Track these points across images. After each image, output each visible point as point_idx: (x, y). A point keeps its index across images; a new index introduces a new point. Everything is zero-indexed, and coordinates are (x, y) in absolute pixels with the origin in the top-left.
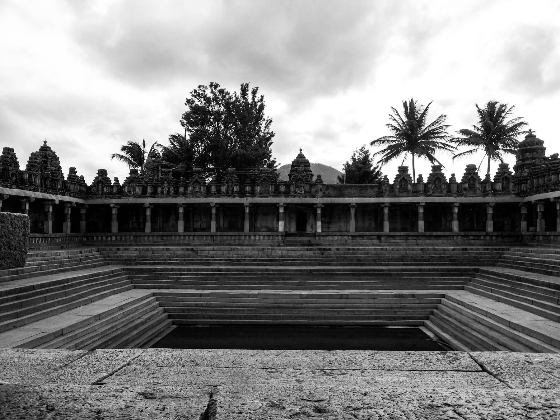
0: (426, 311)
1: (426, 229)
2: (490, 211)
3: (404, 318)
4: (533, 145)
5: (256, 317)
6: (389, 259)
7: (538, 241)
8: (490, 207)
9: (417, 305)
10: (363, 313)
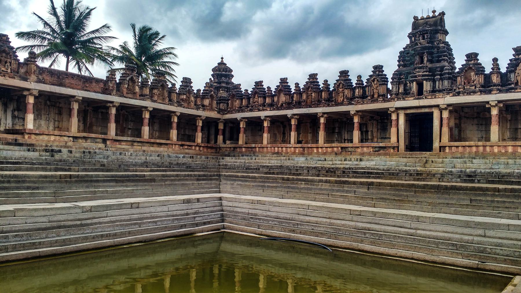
0: (218, 214)
1: (151, 136)
2: (200, 124)
3: (205, 224)
4: (226, 72)
5: (33, 245)
6: (135, 165)
7: (241, 152)
8: (201, 119)
9: (207, 209)
10: (166, 223)
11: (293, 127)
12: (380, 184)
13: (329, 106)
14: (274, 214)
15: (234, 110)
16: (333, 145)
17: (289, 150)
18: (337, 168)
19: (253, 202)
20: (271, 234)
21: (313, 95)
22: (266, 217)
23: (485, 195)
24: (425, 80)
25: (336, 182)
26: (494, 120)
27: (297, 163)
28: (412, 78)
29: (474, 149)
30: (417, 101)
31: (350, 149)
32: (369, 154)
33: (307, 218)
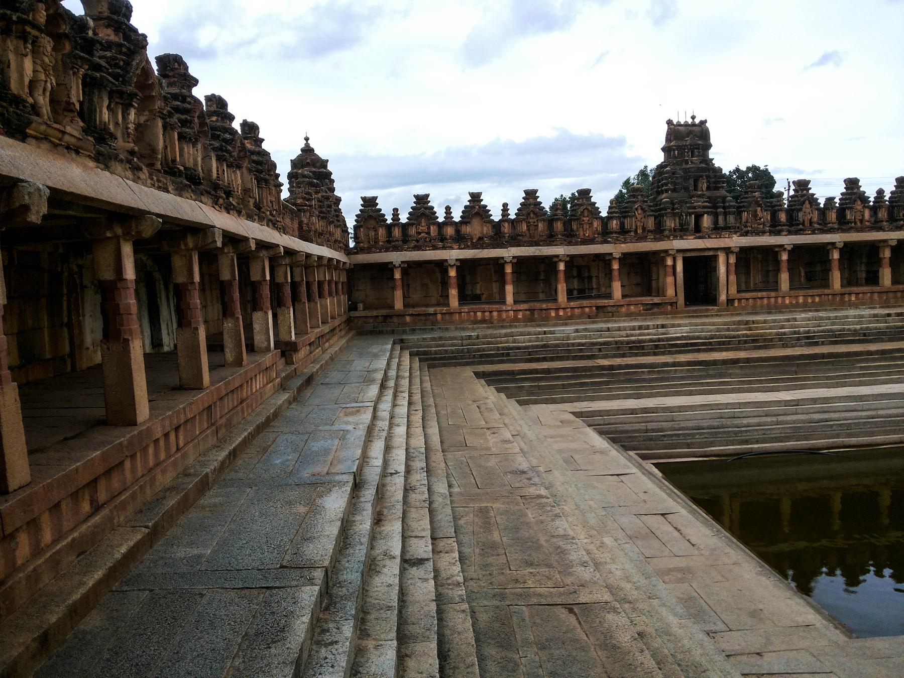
7: (405, 324)
11: (509, 278)
12: (748, 360)
13: (570, 243)
14: (691, 424)
15: (373, 246)
16: (585, 303)
17: (504, 315)
18: (640, 341)
19: (633, 411)
20: (720, 453)
21: (540, 225)
22: (679, 430)
23: (866, 360)
24: (705, 213)
25: (689, 363)
26: (784, 267)
27: (568, 338)
28: (689, 208)
29: (765, 301)
30: (700, 240)
31: (610, 309)
32: (639, 314)
33: (745, 421)
